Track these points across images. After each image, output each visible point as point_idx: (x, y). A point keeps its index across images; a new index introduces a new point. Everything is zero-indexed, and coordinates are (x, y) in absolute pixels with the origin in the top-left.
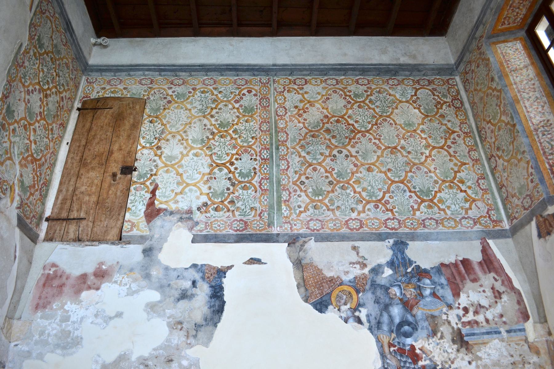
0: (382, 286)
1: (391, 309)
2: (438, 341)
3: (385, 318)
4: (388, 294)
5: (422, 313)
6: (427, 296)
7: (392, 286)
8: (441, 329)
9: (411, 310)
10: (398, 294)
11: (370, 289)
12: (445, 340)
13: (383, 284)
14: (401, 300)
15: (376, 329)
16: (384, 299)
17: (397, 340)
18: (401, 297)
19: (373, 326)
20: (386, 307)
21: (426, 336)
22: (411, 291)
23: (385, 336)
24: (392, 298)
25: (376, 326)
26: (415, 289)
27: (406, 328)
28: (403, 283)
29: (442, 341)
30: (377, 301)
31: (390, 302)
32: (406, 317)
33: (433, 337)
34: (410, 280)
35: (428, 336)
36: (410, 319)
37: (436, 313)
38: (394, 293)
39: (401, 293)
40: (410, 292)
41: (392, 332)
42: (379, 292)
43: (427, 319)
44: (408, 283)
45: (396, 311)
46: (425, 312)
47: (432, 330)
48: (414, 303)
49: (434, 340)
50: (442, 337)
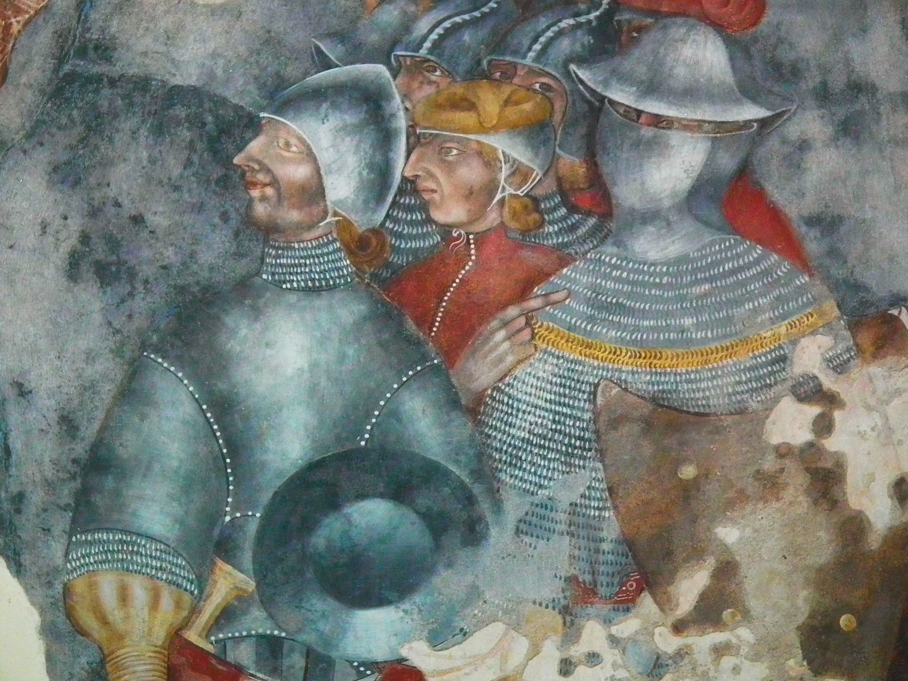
0: (175, 94)
1: (240, 334)
2: (667, 642)
3: (171, 421)
4: (232, 181)
5: (567, 383)
6: (649, 216)
7: (285, 97)
8: (728, 534)
9: (451, 354)
10: (342, 188)
11: (36, 132)
12: (745, 634)
13: (188, 76)
14: (362, 246)
15: (61, 522)
16: (180, 235)
17: (257, 621)
18: (362, 222)
19: (36, 498)
20: (190, 325)
21: (551, 590)
22: (488, 159)
23: (139, 590)
24: (269, 231)
25: (66, 495)
26: (536, 131)
27: (372, 516)
28: (420, 67)
29: (702, 642)
30: (100, 260)
31: (242, 267)
32: (394, 414)
33: (625, 603)
34: (499, 43)
35: (578, 597)
36: (424, 425)
37: (711, 384)
38: (299, 172)
39: (379, 177)
40: (471, 173)
41: (225, 548)
42: (133, 167)
43: (596, 441)
44: (477, 74)
45: (293, 360)
46: (592, 369)
47: (628, 543)
48: (497, 282)
49: (627, 627)
50: (710, 611)
